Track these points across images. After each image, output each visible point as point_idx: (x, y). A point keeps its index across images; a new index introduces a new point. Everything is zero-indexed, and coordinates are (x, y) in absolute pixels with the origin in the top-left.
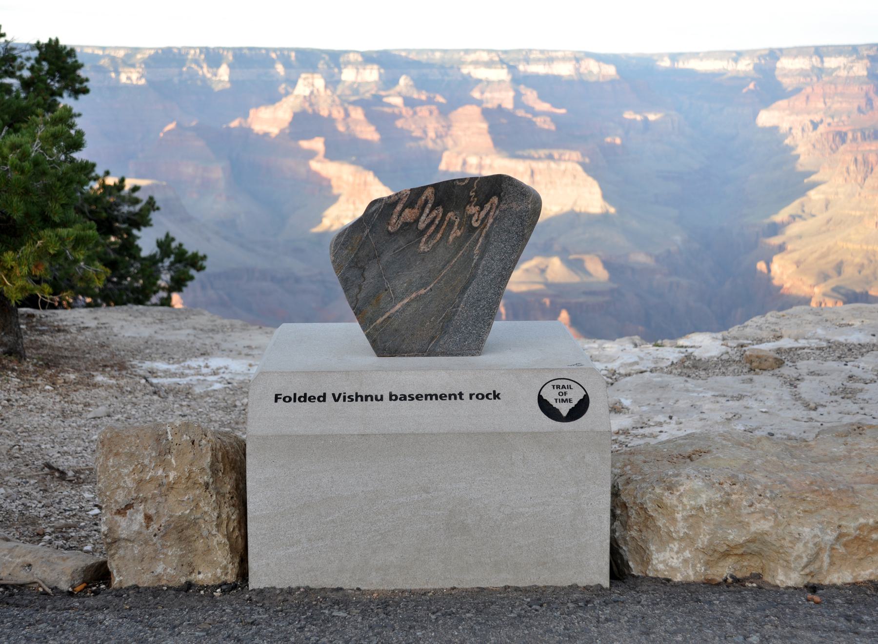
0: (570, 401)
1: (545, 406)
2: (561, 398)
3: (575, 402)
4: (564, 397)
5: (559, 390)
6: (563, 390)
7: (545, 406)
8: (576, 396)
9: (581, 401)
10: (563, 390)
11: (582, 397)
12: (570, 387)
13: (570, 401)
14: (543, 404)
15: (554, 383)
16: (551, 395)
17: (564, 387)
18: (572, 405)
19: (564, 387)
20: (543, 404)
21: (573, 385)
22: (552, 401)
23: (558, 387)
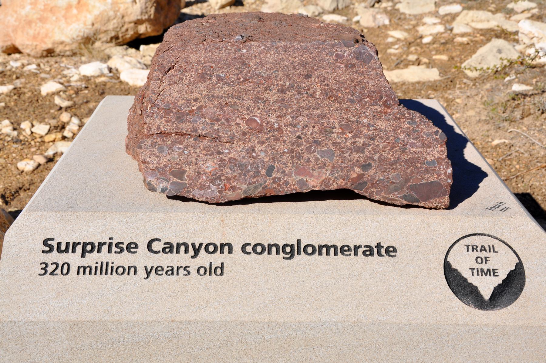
0: (494, 272)
1: (454, 280)
2: (480, 267)
3: (503, 275)
4: (485, 267)
5: (476, 254)
6: (483, 254)
7: (454, 280)
8: (504, 265)
10: (483, 254)
12: (492, 249)
13: (494, 272)
14: (452, 276)
15: (469, 241)
16: (463, 263)
17: (483, 249)
18: (499, 280)
19: (483, 249)
20: (452, 276)
22: (466, 274)
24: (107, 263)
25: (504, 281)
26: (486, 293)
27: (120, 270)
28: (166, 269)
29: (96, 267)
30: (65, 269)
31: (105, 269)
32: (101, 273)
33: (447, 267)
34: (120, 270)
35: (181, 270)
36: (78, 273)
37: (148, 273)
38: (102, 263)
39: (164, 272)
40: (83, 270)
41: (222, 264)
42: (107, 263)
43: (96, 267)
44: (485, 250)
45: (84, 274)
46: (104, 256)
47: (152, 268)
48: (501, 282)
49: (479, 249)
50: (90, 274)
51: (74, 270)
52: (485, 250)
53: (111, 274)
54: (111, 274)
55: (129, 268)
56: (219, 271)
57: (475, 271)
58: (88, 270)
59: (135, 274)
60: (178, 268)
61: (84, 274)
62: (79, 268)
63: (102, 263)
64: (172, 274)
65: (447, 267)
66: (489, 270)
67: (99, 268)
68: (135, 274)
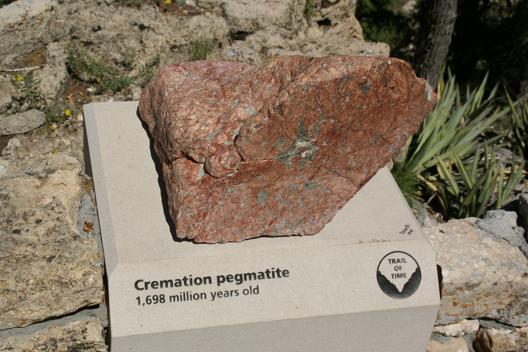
4: (399, 272)
5: (395, 265)
8: (409, 270)
9: (414, 274)
10: (399, 264)
11: (414, 271)
12: (404, 261)
17: (399, 261)
19: (399, 261)
21: (407, 258)
22: (389, 278)
23: (394, 261)
24: (187, 293)
25: (410, 280)
26: (400, 289)
27: (196, 297)
28: (224, 293)
29: (181, 296)
30: (161, 299)
31: (185, 297)
32: (185, 300)
33: (379, 274)
34: (196, 297)
35: (233, 293)
36: (171, 301)
37: (214, 297)
38: (184, 293)
39: (223, 295)
40: (173, 298)
41: (258, 286)
42: (187, 293)
43: (181, 296)
44: (400, 262)
45: (174, 300)
46: (183, 289)
47: (215, 293)
48: (408, 281)
49: (396, 261)
50: (178, 300)
51: (167, 299)
52: (400, 262)
53: (191, 299)
54: (191, 299)
55: (202, 294)
56: (256, 291)
57: (394, 276)
58: (176, 298)
59: (205, 298)
60: (231, 292)
61: (174, 300)
62: (171, 297)
63: (184, 293)
64: (228, 296)
65: (379, 274)
66: (401, 274)
67: (183, 297)
68: (205, 298)
